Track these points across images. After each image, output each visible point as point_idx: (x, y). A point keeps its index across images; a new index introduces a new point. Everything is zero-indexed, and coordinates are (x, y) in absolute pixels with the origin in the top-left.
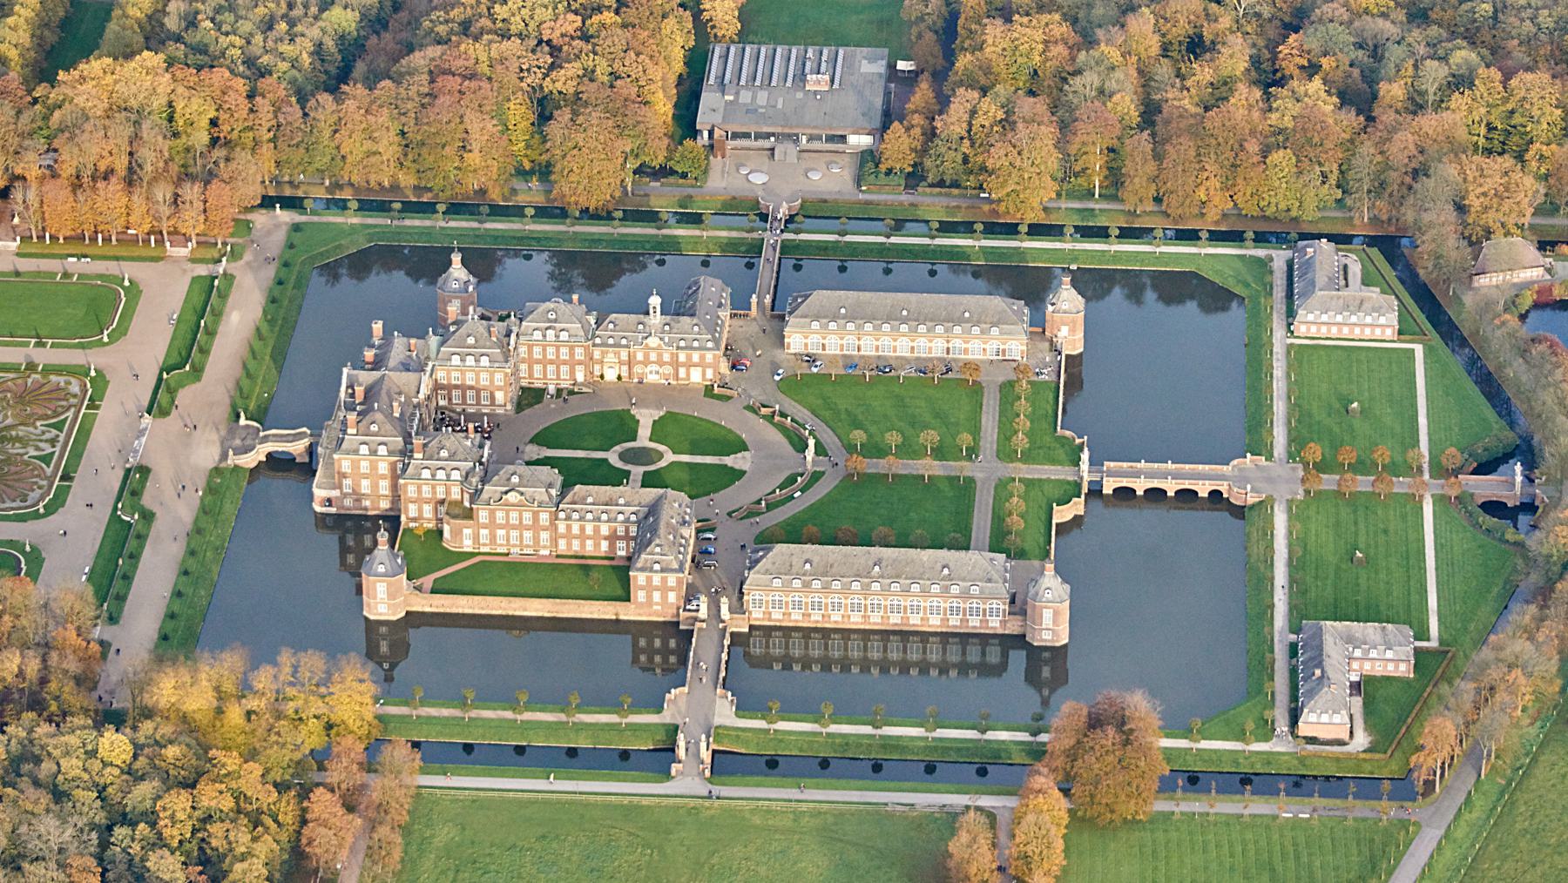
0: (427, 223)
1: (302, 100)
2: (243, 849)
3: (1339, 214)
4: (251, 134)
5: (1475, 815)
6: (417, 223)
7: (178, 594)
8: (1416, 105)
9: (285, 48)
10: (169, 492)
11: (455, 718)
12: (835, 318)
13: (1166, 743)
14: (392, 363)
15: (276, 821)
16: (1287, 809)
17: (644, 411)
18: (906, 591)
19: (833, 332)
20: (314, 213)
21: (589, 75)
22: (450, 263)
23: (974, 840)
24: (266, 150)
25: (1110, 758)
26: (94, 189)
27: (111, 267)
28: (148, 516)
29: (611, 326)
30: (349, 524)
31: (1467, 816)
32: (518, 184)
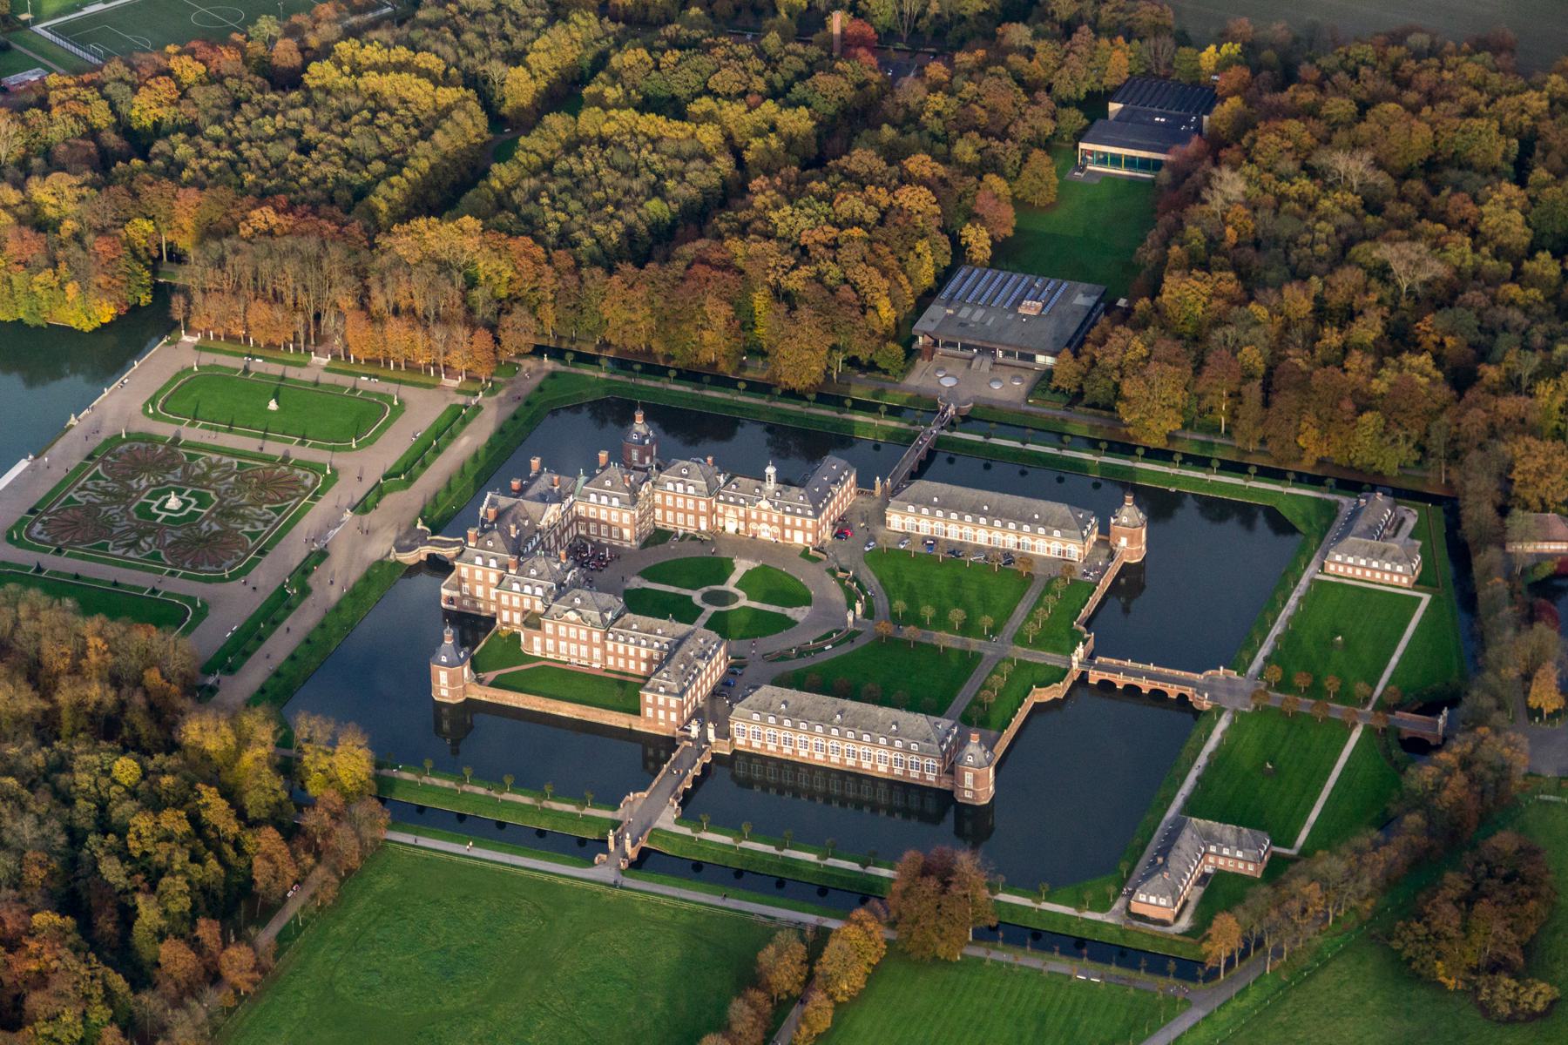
5: (1244, 1003)
6: (651, 383)
7: (293, 658)
8: (1513, 385)
9: (599, 228)
12: (929, 504)
14: (531, 492)
16: (1083, 973)
18: (859, 739)
19: (925, 517)
21: (819, 278)
22: (633, 419)
27: (392, 388)
30: (467, 621)
31: (1236, 1004)
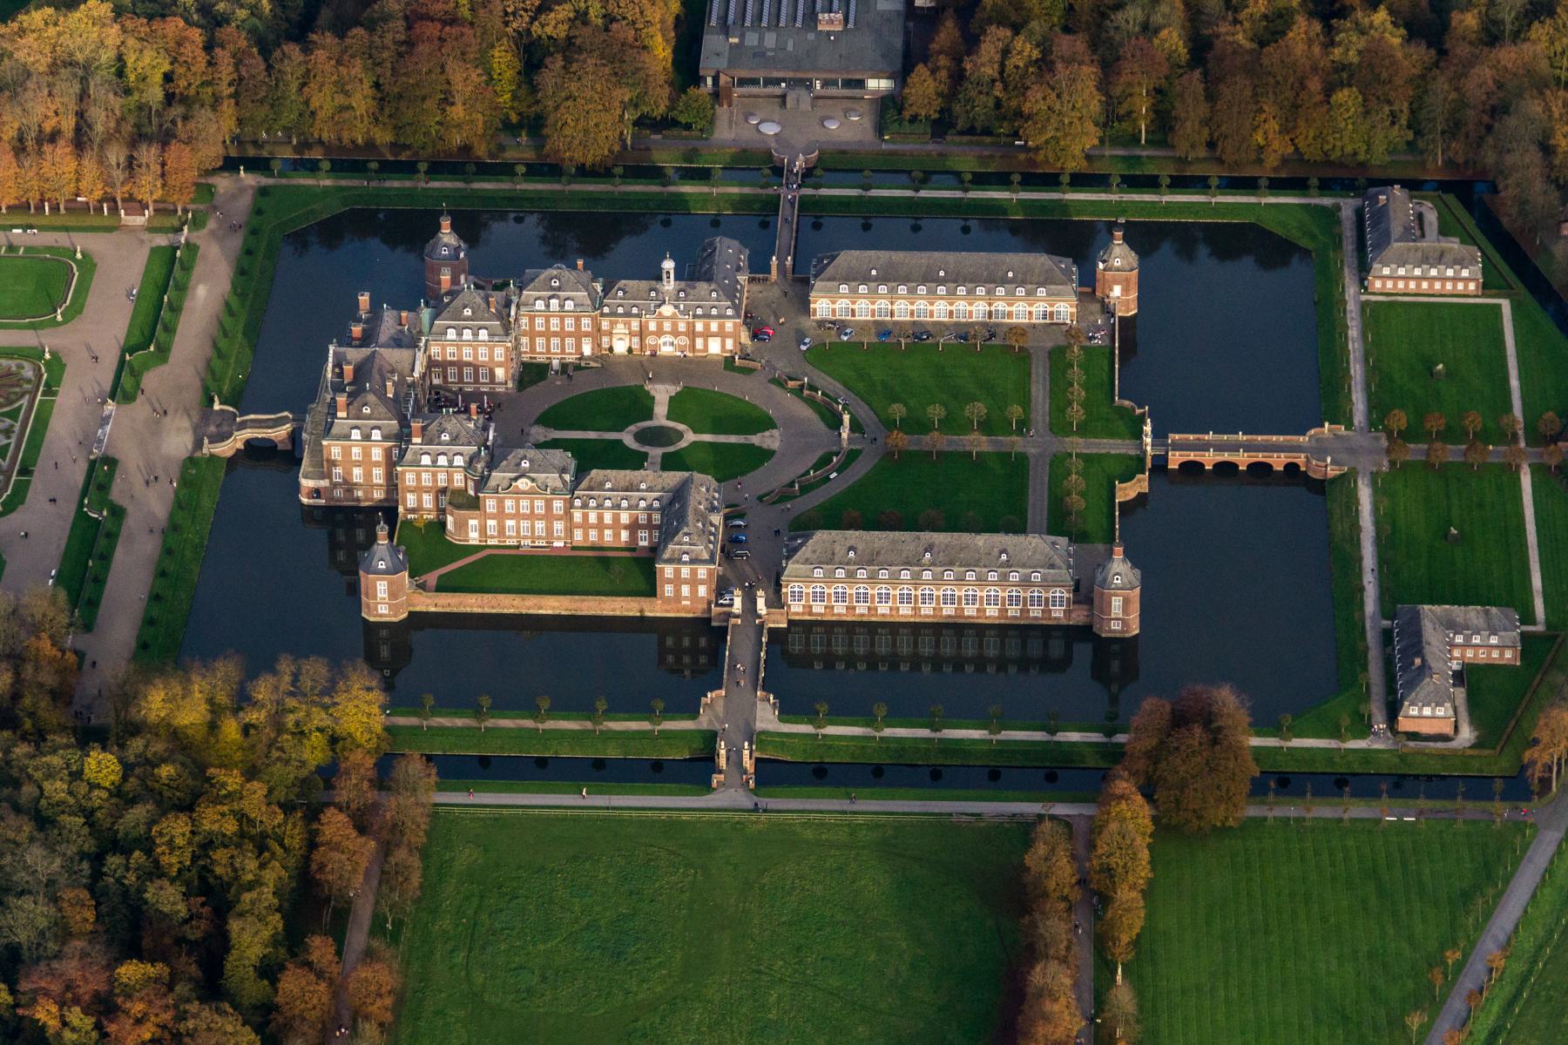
0: (408, 184)
1: (265, 52)
2: (250, 877)
3: (1410, 158)
4: (209, 90)
6: (396, 184)
7: (156, 598)
8: (1492, 35)
10: (138, 481)
11: (469, 728)
12: (866, 279)
13: (1255, 741)
14: (383, 338)
15: (282, 845)
16: (1391, 814)
17: (659, 387)
20: (281, 175)
22: (438, 228)
23: (1053, 850)
24: (228, 107)
25: (1199, 759)
26: (40, 153)
27: (61, 239)
28: (118, 513)
29: (620, 294)
30: (339, 517)
32: (504, 138)
